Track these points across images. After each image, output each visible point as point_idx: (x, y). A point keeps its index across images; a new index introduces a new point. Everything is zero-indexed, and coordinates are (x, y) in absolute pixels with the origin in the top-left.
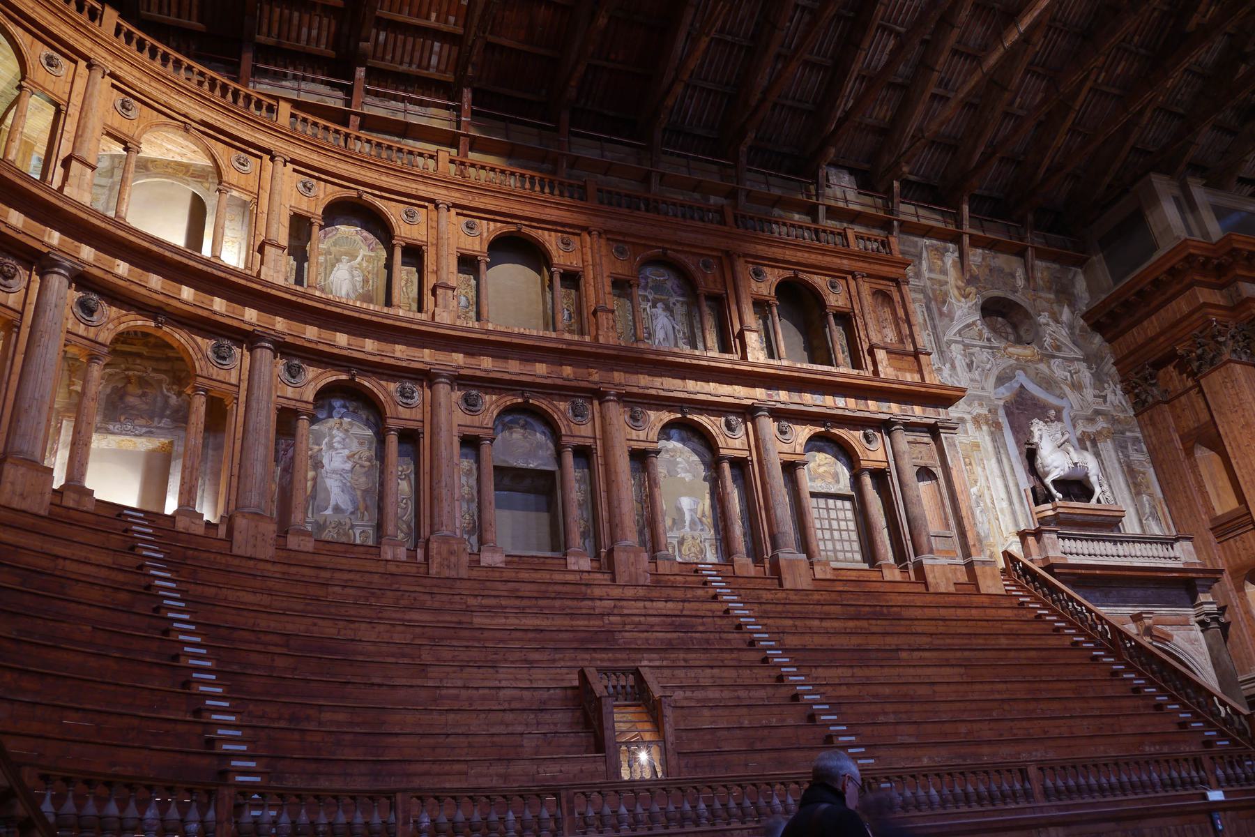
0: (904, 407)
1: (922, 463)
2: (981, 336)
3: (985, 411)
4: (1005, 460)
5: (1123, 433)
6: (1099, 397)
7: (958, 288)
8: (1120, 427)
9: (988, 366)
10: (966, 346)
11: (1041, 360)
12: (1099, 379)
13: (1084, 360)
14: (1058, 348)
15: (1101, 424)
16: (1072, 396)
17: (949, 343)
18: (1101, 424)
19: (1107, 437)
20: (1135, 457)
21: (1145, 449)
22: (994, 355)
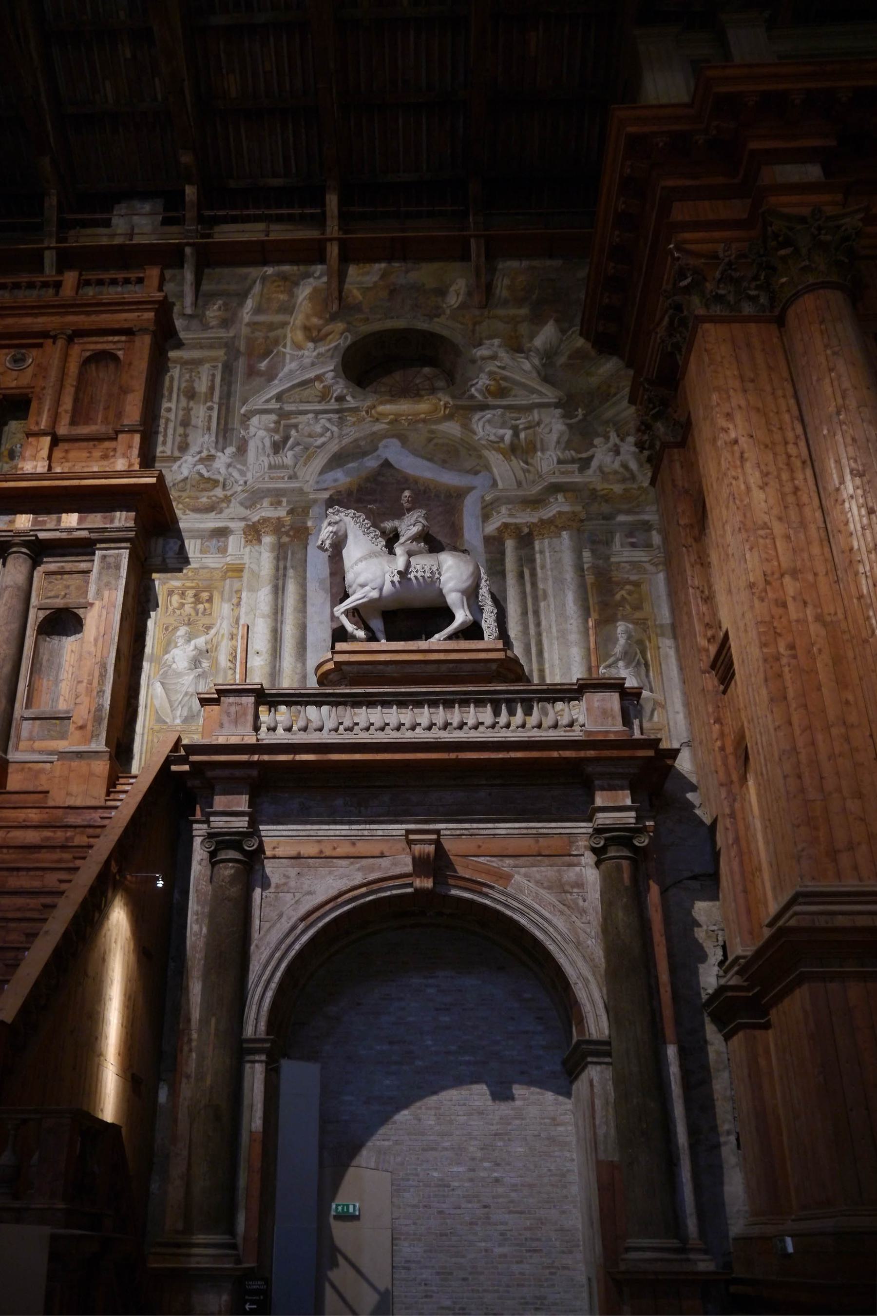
0: (41, 518)
1: (59, 603)
2: (324, 396)
3: (281, 512)
4: (291, 588)
5: (608, 517)
6: (573, 461)
7: (306, 329)
8: (605, 508)
9: (323, 439)
10: (283, 415)
11: (449, 417)
12: (582, 435)
13: (557, 406)
14: (502, 393)
15: (559, 505)
16: (503, 469)
17: (247, 417)
18: (559, 505)
19: (564, 528)
20: (622, 554)
21: (656, 538)
22: (341, 422)
